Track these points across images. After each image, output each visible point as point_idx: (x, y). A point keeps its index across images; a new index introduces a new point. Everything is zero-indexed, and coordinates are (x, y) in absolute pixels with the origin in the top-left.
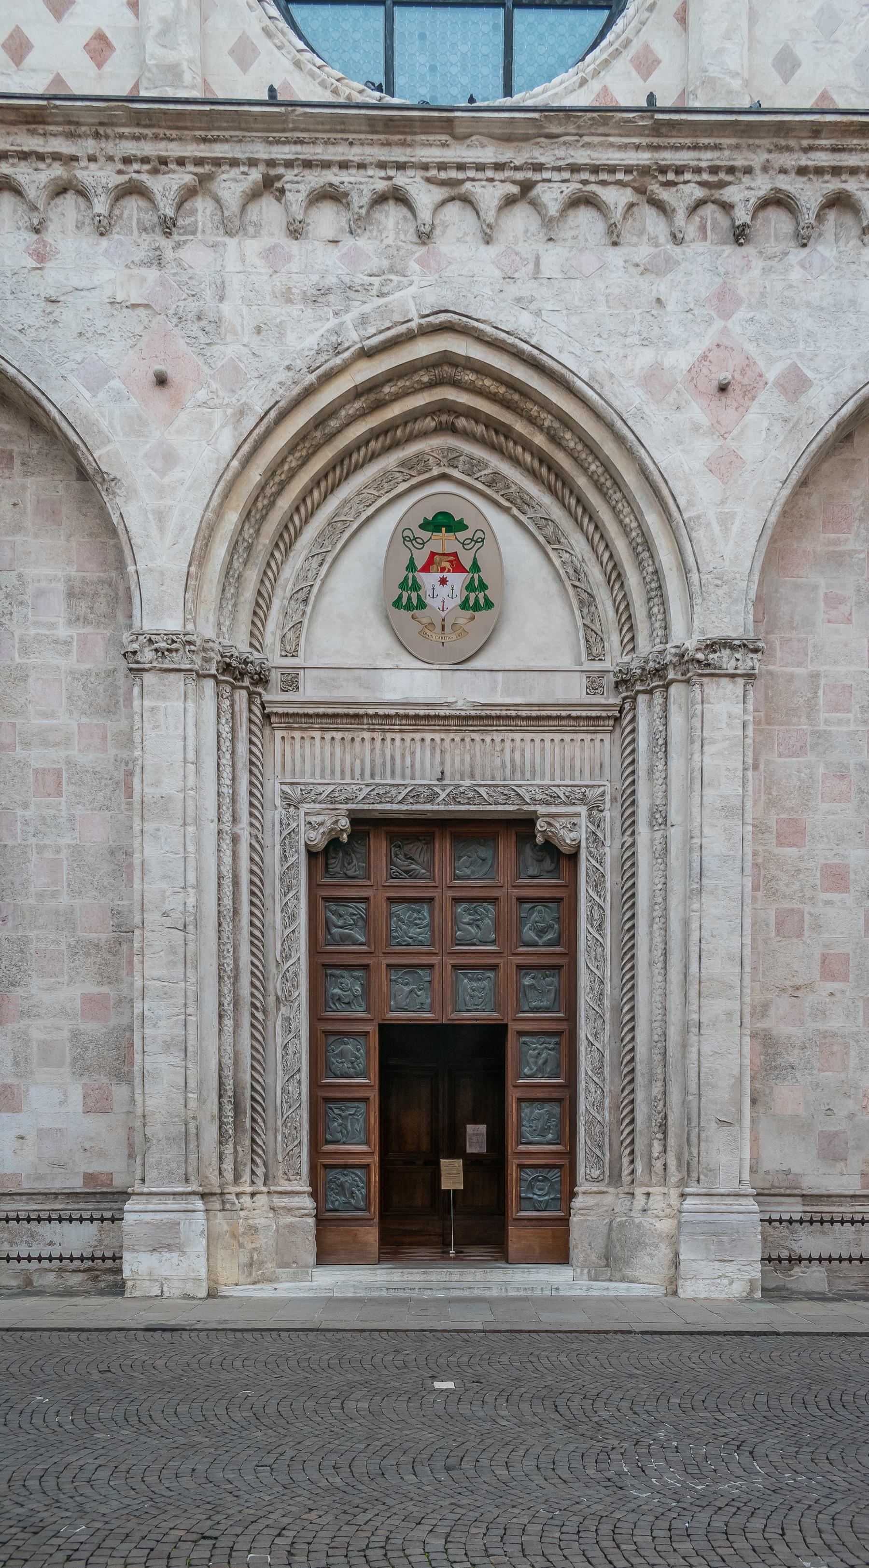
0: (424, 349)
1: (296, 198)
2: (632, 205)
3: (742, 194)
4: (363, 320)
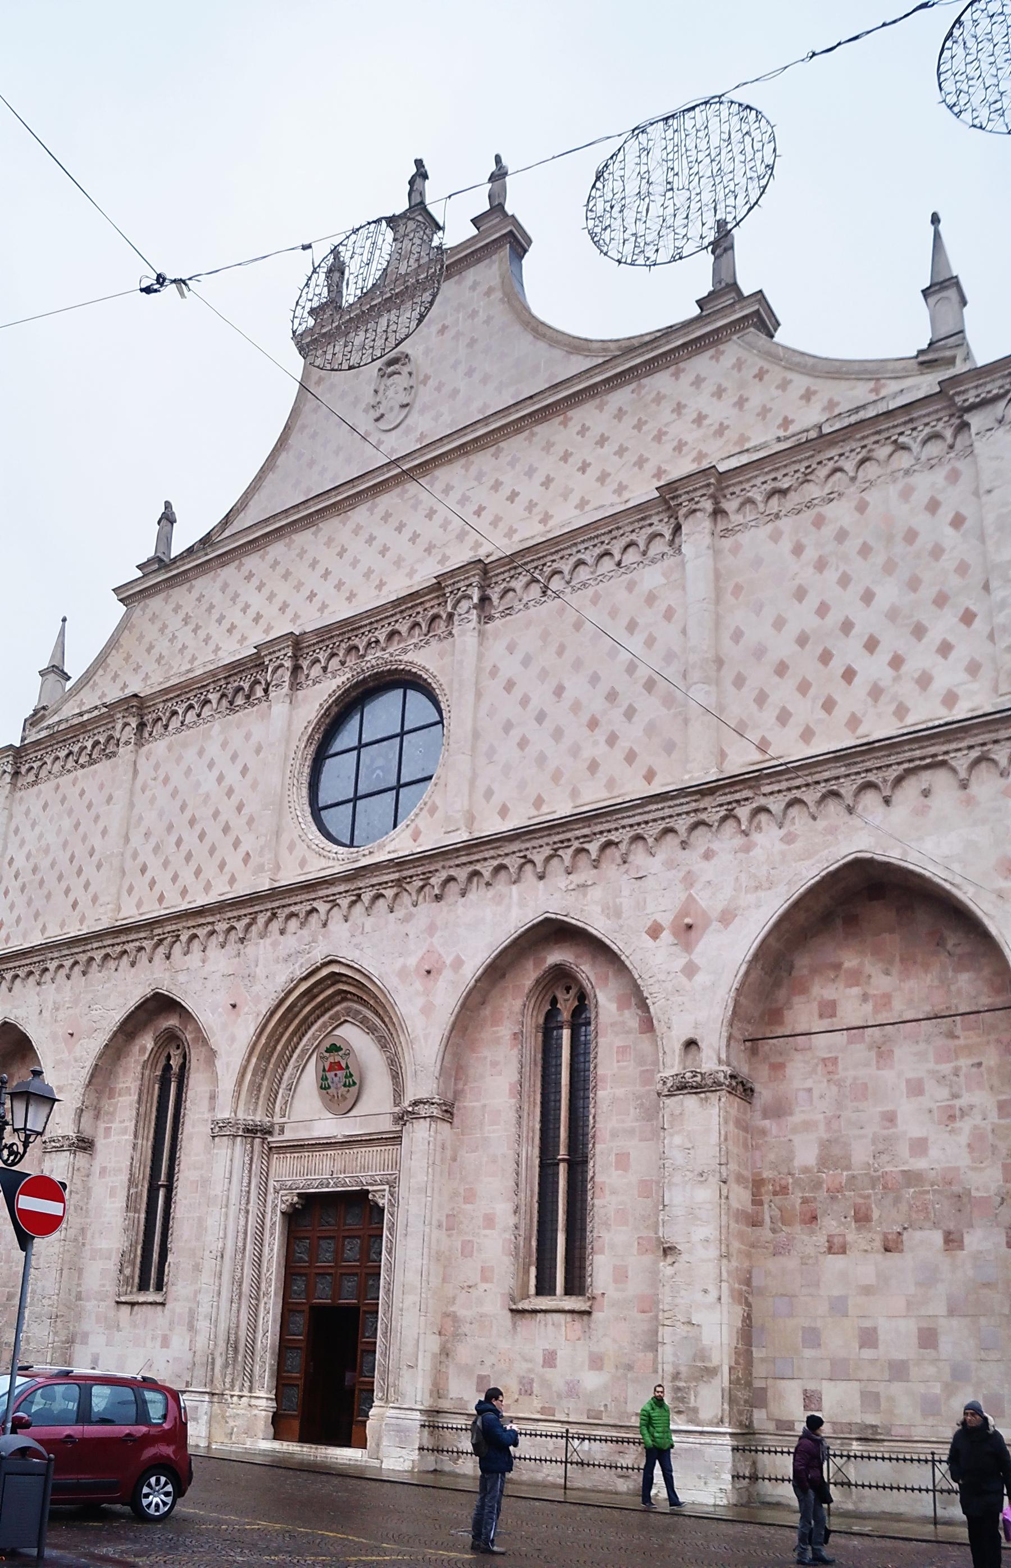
0: (324, 972)
1: (281, 919)
2: (397, 895)
3: (436, 881)
4: (301, 966)
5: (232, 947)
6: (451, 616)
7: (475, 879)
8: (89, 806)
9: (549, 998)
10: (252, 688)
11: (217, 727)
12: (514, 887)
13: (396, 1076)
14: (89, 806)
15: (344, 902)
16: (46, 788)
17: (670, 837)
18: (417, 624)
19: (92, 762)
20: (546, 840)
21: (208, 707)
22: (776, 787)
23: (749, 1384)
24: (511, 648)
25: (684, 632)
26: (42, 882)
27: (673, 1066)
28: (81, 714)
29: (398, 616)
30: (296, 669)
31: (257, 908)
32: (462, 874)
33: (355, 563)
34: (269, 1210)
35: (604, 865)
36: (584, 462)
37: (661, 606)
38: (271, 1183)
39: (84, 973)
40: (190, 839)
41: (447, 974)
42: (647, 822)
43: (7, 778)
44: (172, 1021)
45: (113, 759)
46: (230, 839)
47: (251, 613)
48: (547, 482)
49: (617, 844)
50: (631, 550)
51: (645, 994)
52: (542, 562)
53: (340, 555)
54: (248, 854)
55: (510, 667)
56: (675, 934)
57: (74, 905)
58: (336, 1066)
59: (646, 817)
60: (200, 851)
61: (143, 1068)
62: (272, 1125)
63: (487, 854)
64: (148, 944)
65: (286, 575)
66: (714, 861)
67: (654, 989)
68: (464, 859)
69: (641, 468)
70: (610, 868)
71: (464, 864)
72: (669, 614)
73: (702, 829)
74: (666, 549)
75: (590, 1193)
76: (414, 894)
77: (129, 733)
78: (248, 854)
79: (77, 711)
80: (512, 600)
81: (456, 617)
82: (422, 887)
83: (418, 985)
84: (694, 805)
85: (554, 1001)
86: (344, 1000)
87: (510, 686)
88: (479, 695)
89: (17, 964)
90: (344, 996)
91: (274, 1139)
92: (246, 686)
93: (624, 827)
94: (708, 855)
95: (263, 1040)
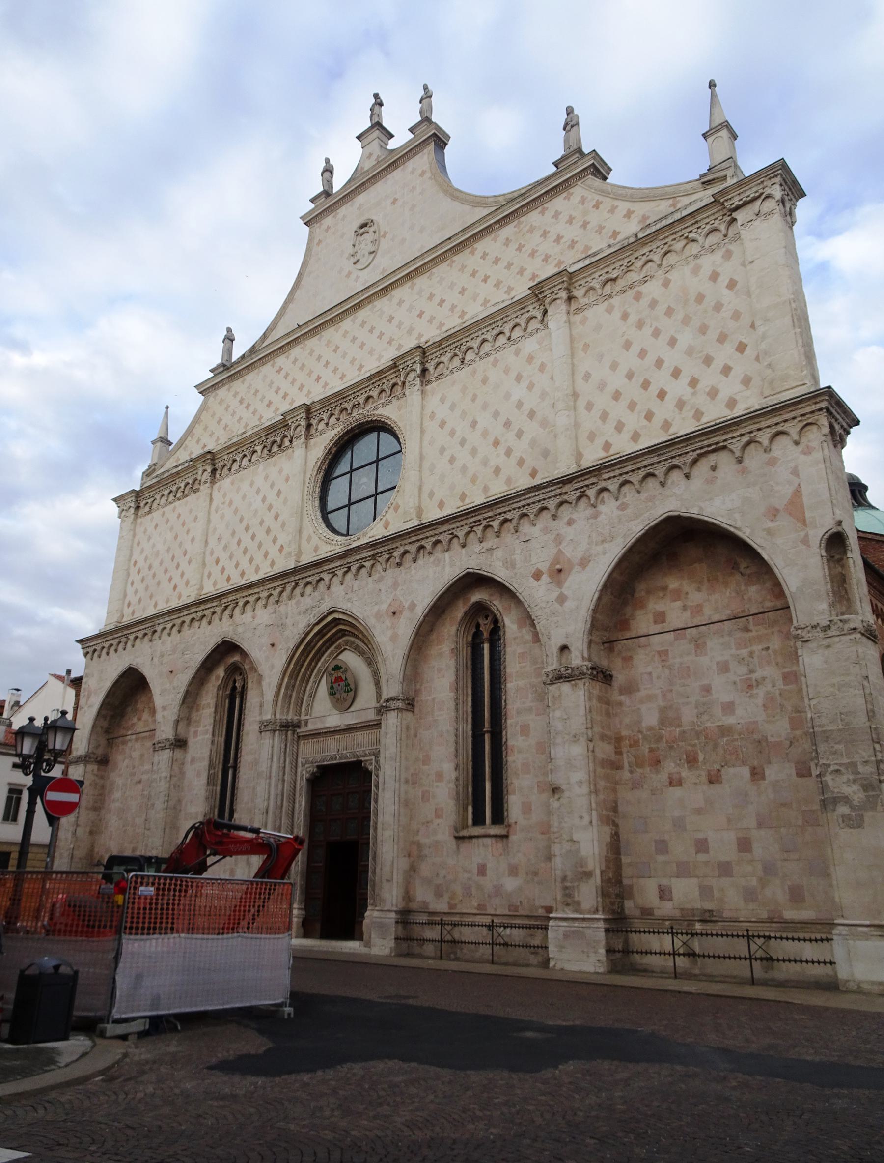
0: (329, 618)
2: (373, 565)
3: (397, 554)
5: (271, 608)
6: (404, 383)
7: (422, 551)
8: (184, 524)
9: (474, 624)
10: (282, 440)
11: (261, 466)
12: (447, 555)
13: (377, 683)
14: (184, 524)
15: (340, 573)
16: (156, 515)
17: (545, 512)
18: (383, 391)
19: (185, 496)
20: (465, 522)
21: (255, 455)
22: (611, 474)
23: (619, 882)
24: (443, 400)
25: (552, 378)
26: (154, 576)
27: (553, 664)
28: (177, 467)
29: (371, 387)
30: (309, 426)
31: (285, 581)
32: (413, 548)
33: (344, 355)
34: (298, 778)
35: (503, 535)
36: (485, 275)
37: (537, 363)
38: (300, 760)
39: (179, 631)
40: (246, 540)
41: (406, 614)
42: (529, 505)
43: (132, 510)
44: (236, 658)
45: (198, 493)
46: (271, 537)
47: (281, 393)
48: (463, 291)
49: (511, 520)
50: (517, 329)
51: (533, 617)
52: (460, 343)
53: (335, 351)
54: (282, 546)
55: (442, 412)
56: (551, 576)
57: (175, 588)
58: (339, 679)
59: (528, 501)
60: (252, 546)
61: (218, 690)
62: (299, 721)
63: (428, 534)
64: (218, 610)
65: (302, 368)
66: (574, 526)
67: (539, 613)
68: (414, 539)
69: (521, 275)
70: (508, 537)
71: (414, 542)
72: (542, 368)
73: (565, 506)
74: (539, 326)
75: (504, 753)
76: (384, 563)
77: (207, 476)
78: (282, 546)
79: (175, 464)
80: (442, 369)
81: (407, 384)
82: (388, 559)
83: (388, 623)
84: (559, 491)
85: (478, 626)
86: (344, 635)
87: (443, 424)
88: (423, 432)
89: (137, 629)
90: (343, 633)
91: (302, 730)
92: (278, 439)
93: (514, 509)
94: (570, 523)
95: (292, 666)
